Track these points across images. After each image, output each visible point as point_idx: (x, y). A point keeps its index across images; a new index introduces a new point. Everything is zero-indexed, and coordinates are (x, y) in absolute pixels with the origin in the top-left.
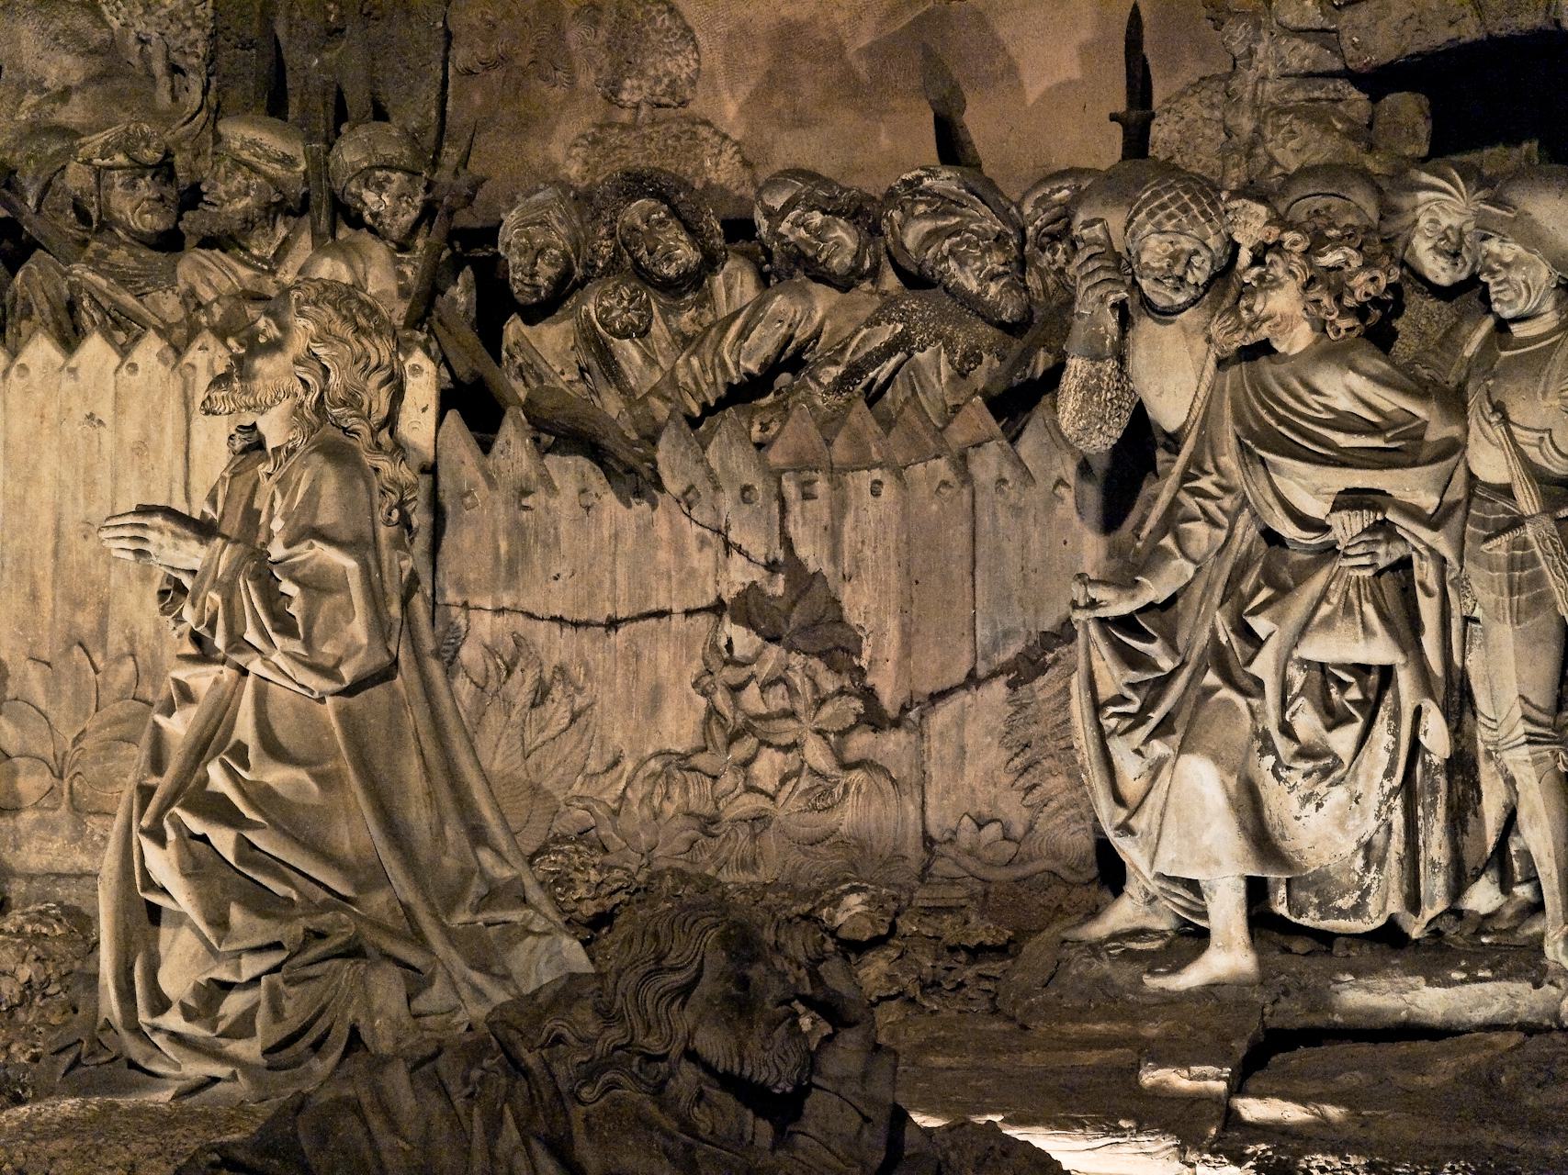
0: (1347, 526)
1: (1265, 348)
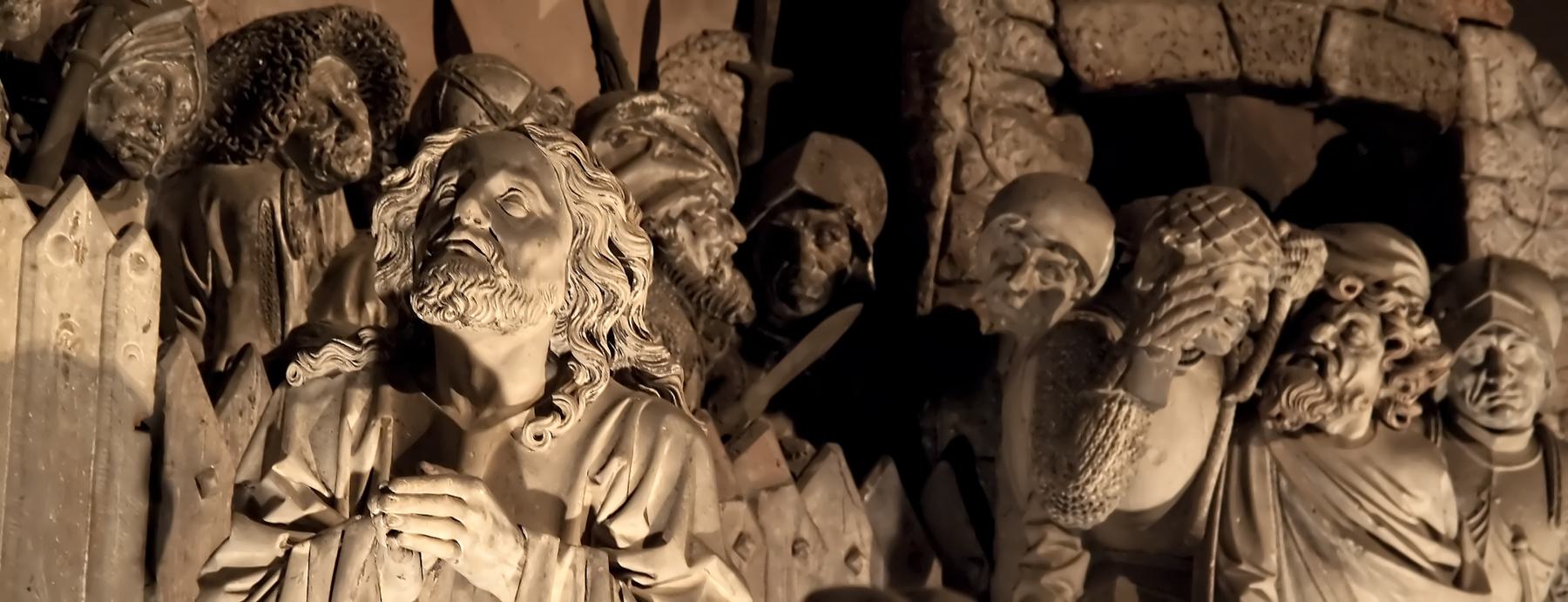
1: (1314, 429)
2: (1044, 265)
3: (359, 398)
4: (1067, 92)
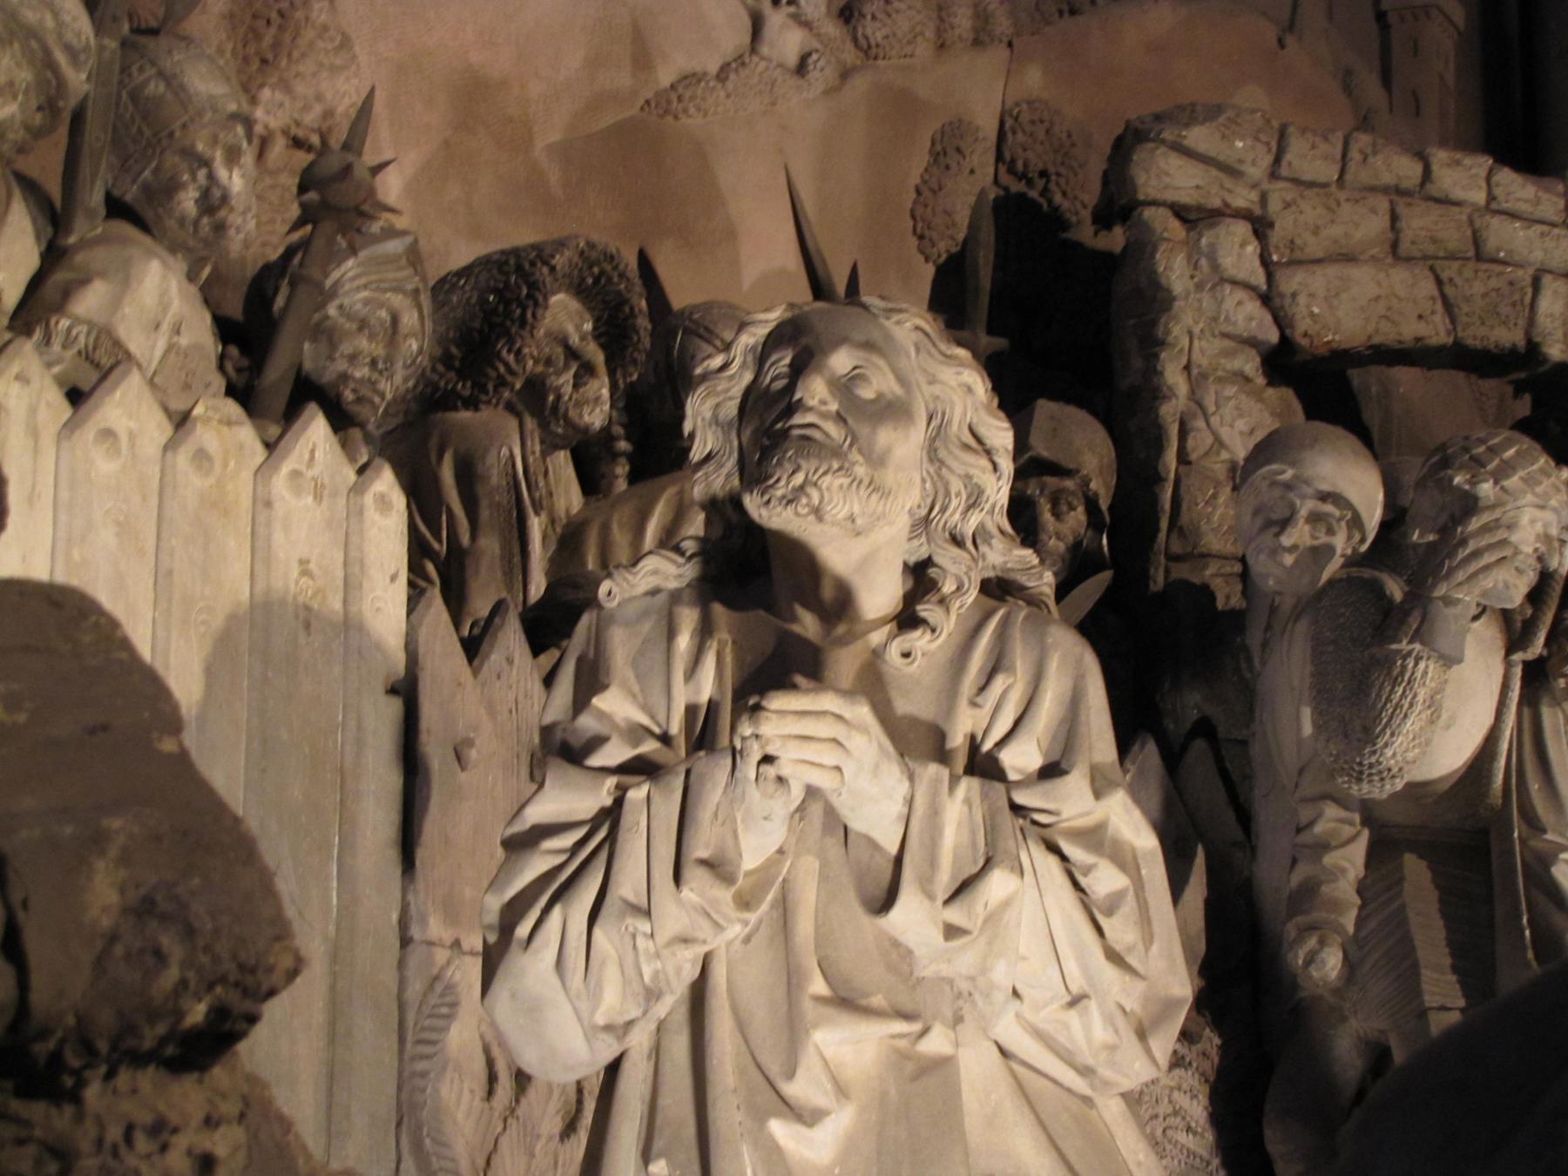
2: (1315, 518)
3: (688, 619)
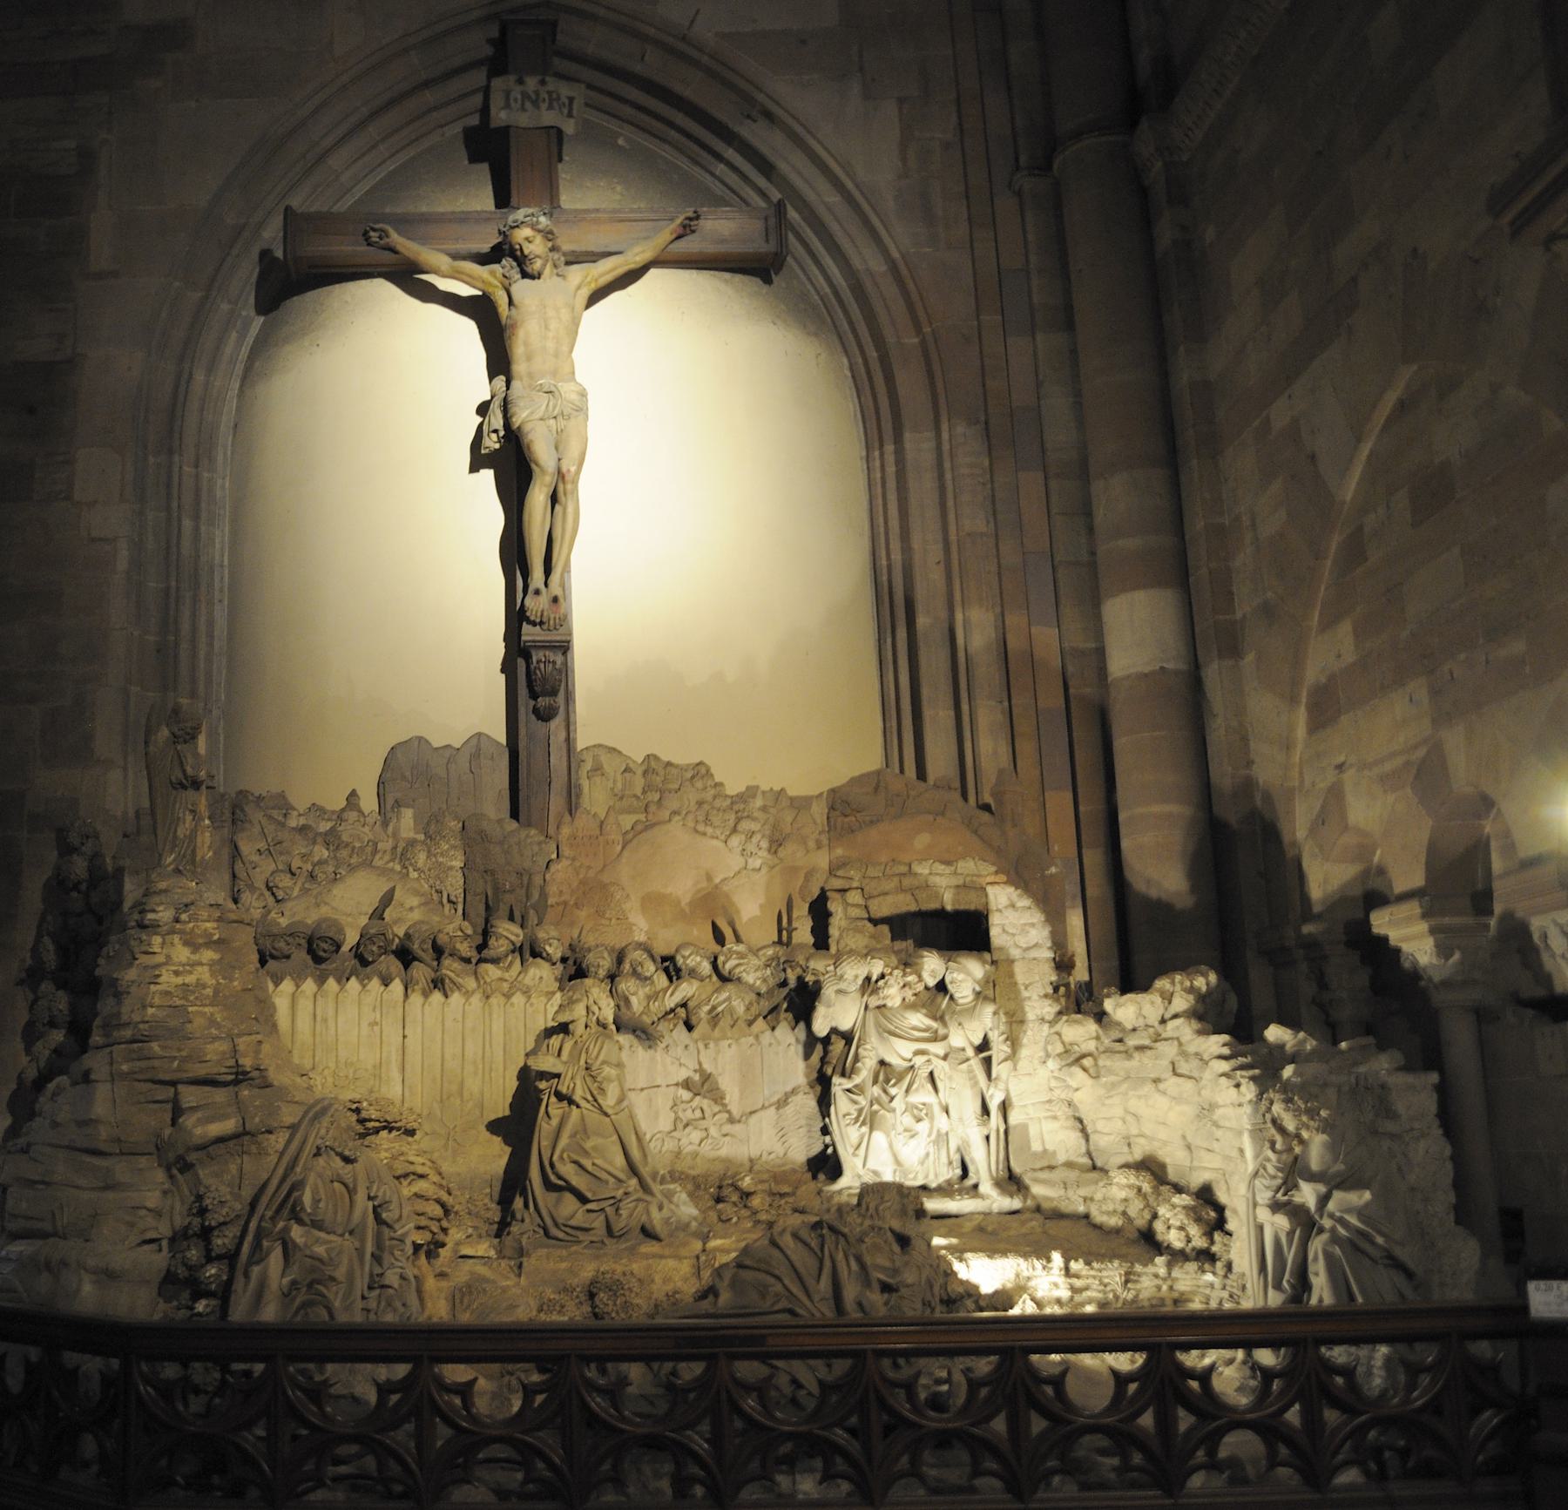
0: (919, 1060)
4: (875, 922)
